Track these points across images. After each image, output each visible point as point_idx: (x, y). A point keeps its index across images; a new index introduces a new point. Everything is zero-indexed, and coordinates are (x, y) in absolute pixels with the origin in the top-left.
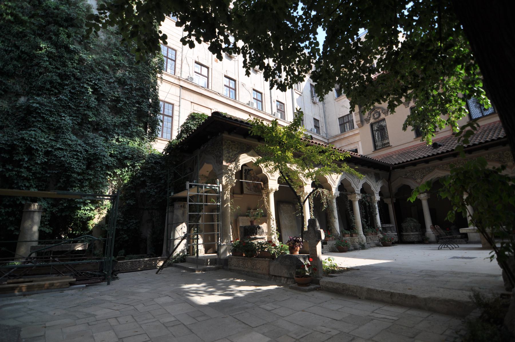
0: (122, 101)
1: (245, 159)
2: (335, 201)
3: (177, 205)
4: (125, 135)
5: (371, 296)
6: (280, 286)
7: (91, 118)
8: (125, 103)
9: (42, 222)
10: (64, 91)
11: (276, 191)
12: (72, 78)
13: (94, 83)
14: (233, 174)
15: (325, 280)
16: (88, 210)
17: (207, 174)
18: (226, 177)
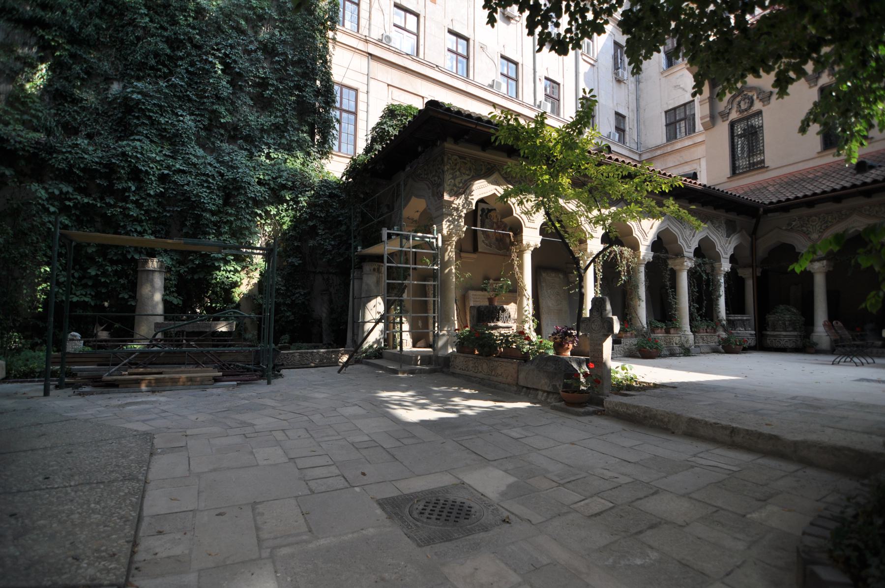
1: (482, 189)
2: (642, 269)
3: (367, 267)
4: (280, 147)
5: (694, 430)
6: (535, 403)
7: (224, 118)
8: (277, 89)
9: (166, 288)
10: (178, 70)
11: (535, 249)
12: (189, 46)
13: (225, 54)
14: (460, 217)
15: (613, 400)
17: (416, 216)
18: (448, 221)
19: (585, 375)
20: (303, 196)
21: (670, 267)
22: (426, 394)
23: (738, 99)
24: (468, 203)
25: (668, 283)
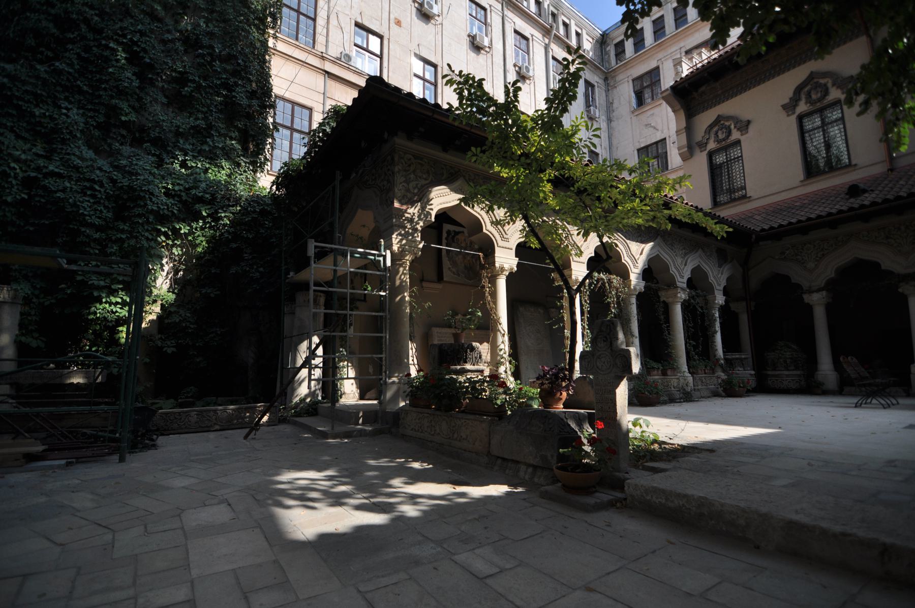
0: (191, 81)
1: (443, 198)
2: (634, 300)
3: (300, 298)
4: (198, 154)
7: (126, 115)
8: (199, 87)
9: (21, 326)
10: (67, 54)
11: (511, 273)
12: (84, 28)
13: (131, 40)
14: (416, 230)
15: (639, 480)
16: (117, 303)
18: (400, 234)
19: (592, 441)
20: (225, 212)
21: (662, 299)
22: (352, 474)
23: (715, 129)
24: (424, 213)
25: (662, 317)
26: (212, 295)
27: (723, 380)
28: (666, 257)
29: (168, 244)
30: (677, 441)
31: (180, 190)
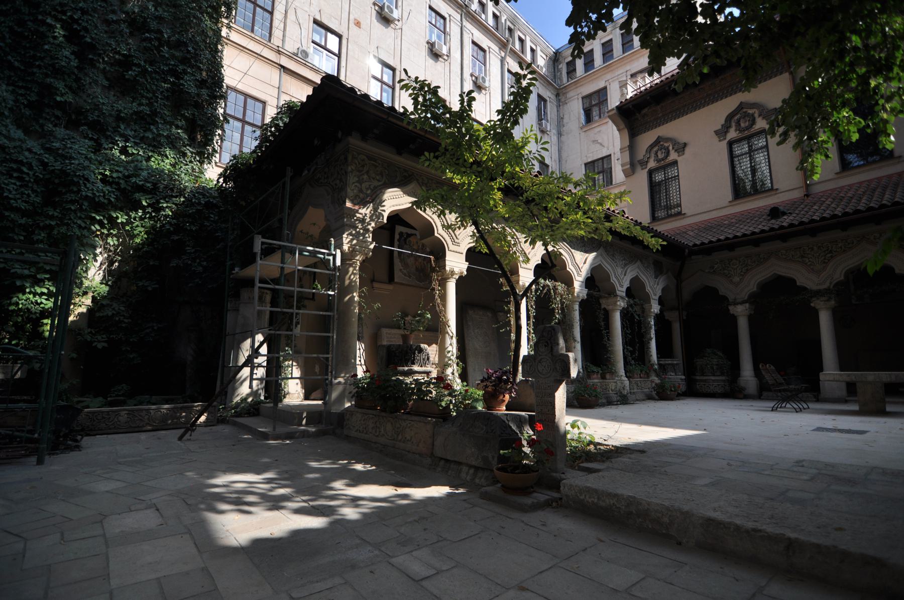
0: (136, 65)
1: (395, 200)
2: (577, 307)
3: (245, 294)
4: (141, 141)
6: (456, 487)
7: (62, 95)
8: (144, 72)
11: (461, 277)
13: (71, 17)
15: (574, 480)
16: (42, 294)
18: (351, 234)
19: (531, 443)
20: (167, 202)
23: (656, 149)
24: (376, 215)
25: (602, 324)
26: (150, 289)
27: (656, 384)
28: (607, 267)
29: (102, 233)
30: (611, 442)
31: (119, 177)
